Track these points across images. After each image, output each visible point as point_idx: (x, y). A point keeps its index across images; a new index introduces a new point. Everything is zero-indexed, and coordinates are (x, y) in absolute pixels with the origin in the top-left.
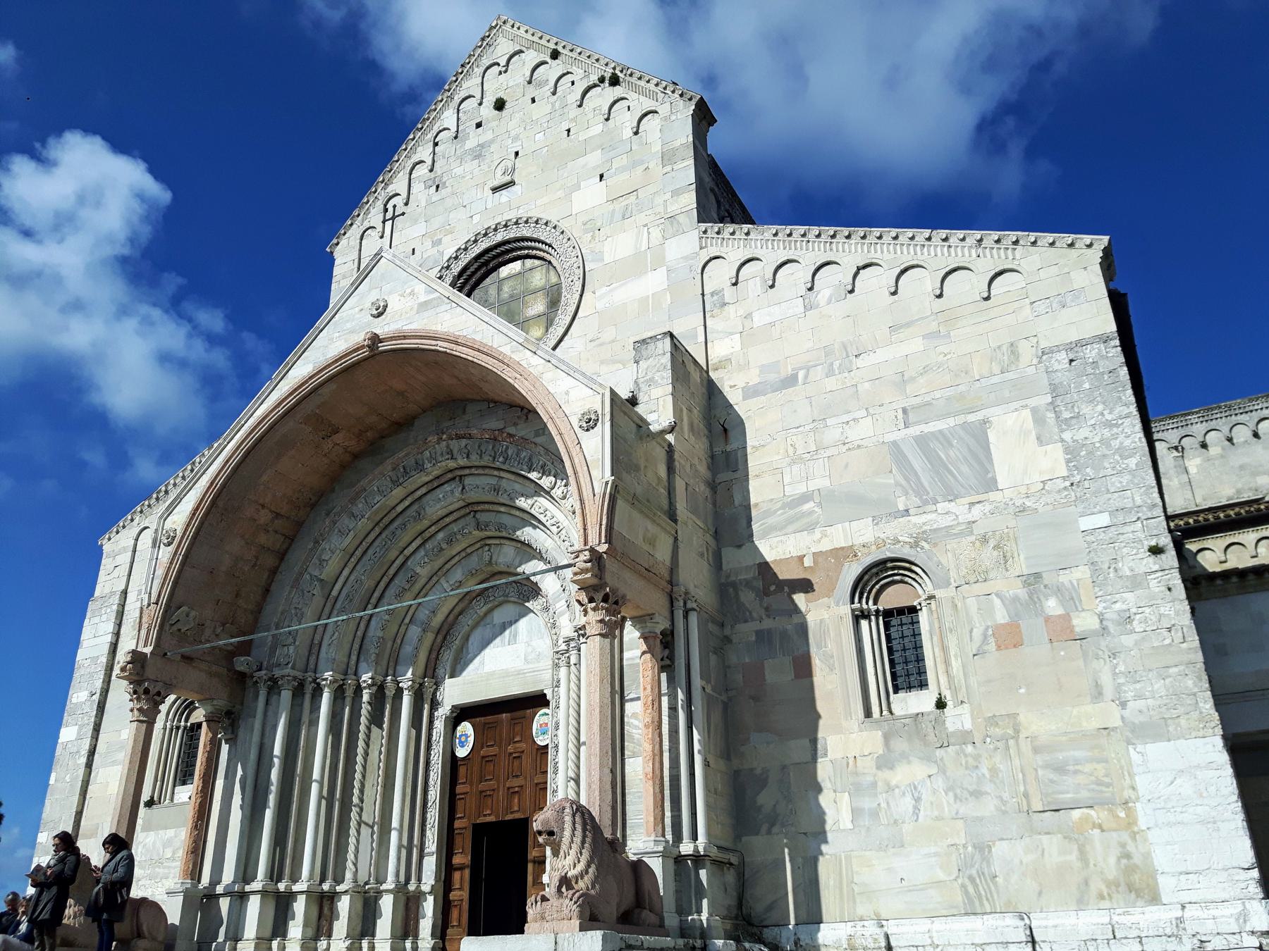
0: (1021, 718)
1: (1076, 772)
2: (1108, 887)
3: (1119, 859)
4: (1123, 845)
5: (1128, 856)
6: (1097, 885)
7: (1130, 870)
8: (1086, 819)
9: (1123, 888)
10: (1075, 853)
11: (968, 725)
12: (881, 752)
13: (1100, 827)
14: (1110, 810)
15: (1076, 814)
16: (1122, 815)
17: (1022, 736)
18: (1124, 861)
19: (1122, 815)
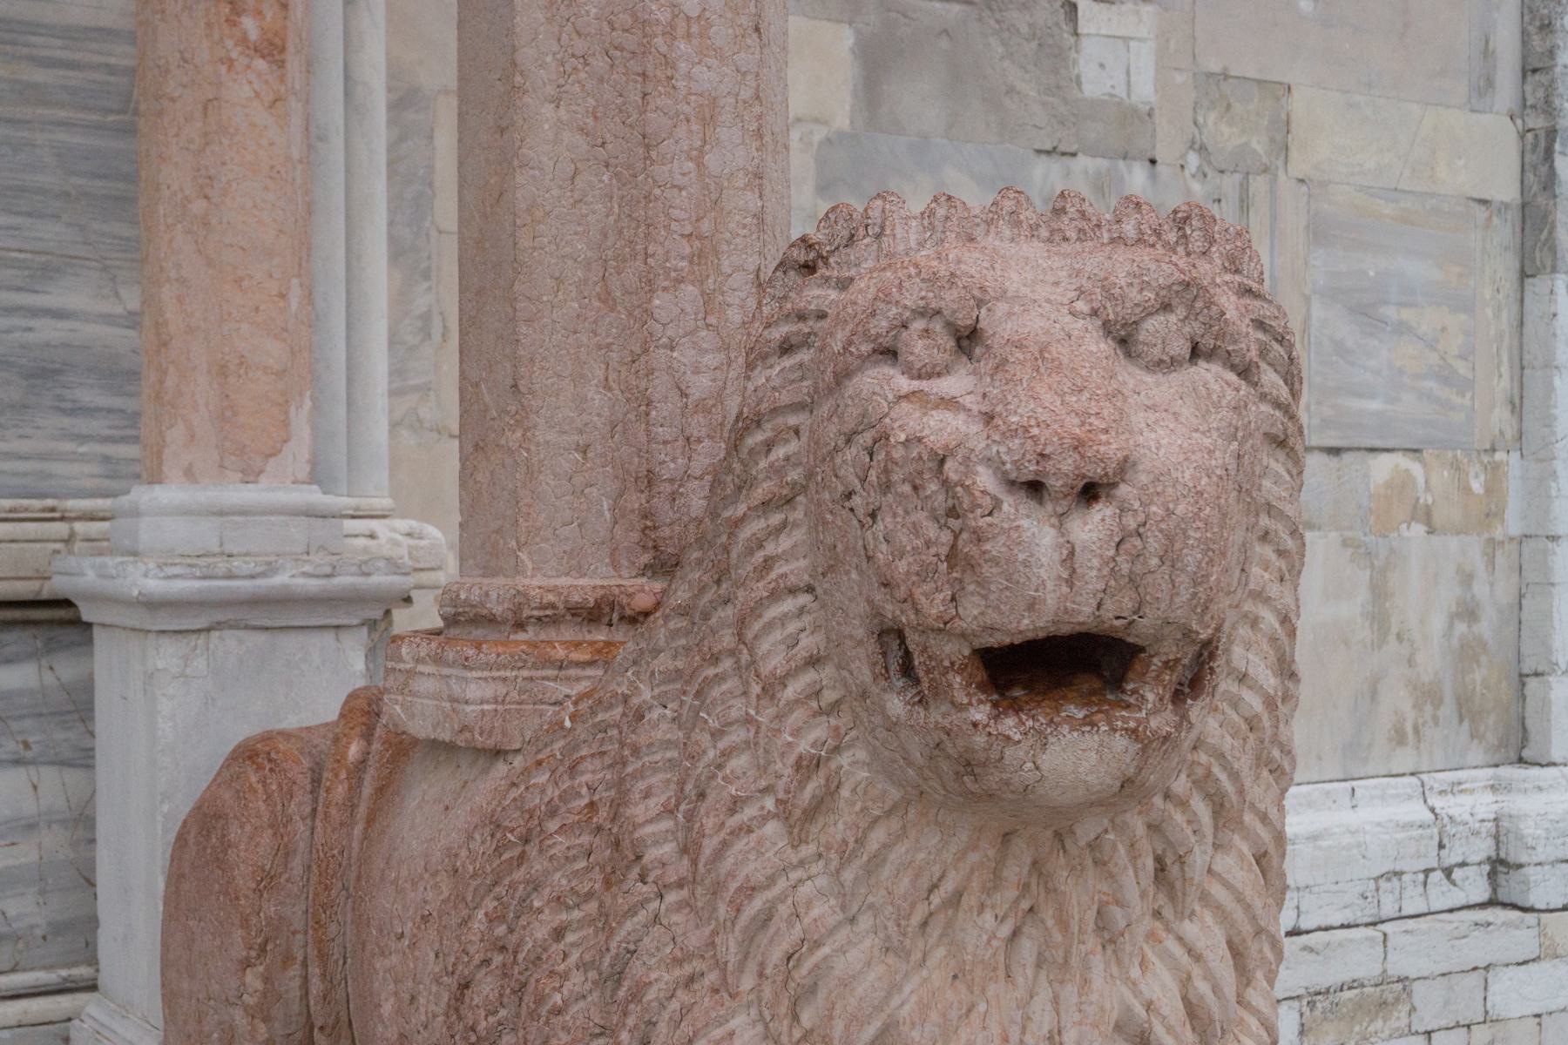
0: (1298, 105)
1: (1402, 329)
2: (1417, 706)
3: (1453, 617)
4: (1467, 579)
5: (1469, 612)
6: (1397, 700)
7: (1467, 654)
8: (1402, 483)
9: (1448, 710)
10: (1363, 595)
11: (1144, 90)
12: (842, 121)
13: (1426, 516)
14: (1456, 466)
15: (1382, 468)
16: (1477, 486)
17: (1298, 166)
18: (1461, 628)
19: (1477, 486)
